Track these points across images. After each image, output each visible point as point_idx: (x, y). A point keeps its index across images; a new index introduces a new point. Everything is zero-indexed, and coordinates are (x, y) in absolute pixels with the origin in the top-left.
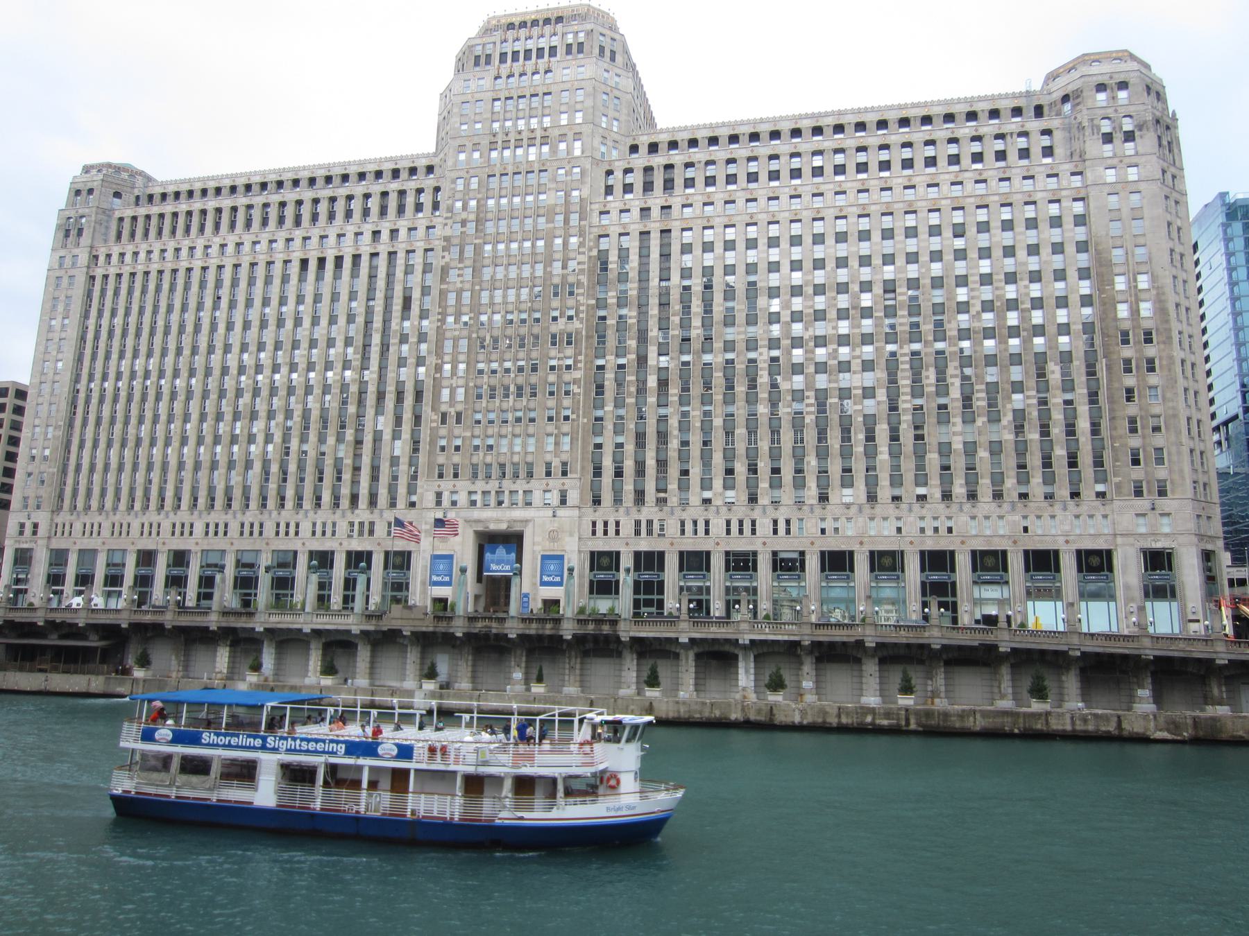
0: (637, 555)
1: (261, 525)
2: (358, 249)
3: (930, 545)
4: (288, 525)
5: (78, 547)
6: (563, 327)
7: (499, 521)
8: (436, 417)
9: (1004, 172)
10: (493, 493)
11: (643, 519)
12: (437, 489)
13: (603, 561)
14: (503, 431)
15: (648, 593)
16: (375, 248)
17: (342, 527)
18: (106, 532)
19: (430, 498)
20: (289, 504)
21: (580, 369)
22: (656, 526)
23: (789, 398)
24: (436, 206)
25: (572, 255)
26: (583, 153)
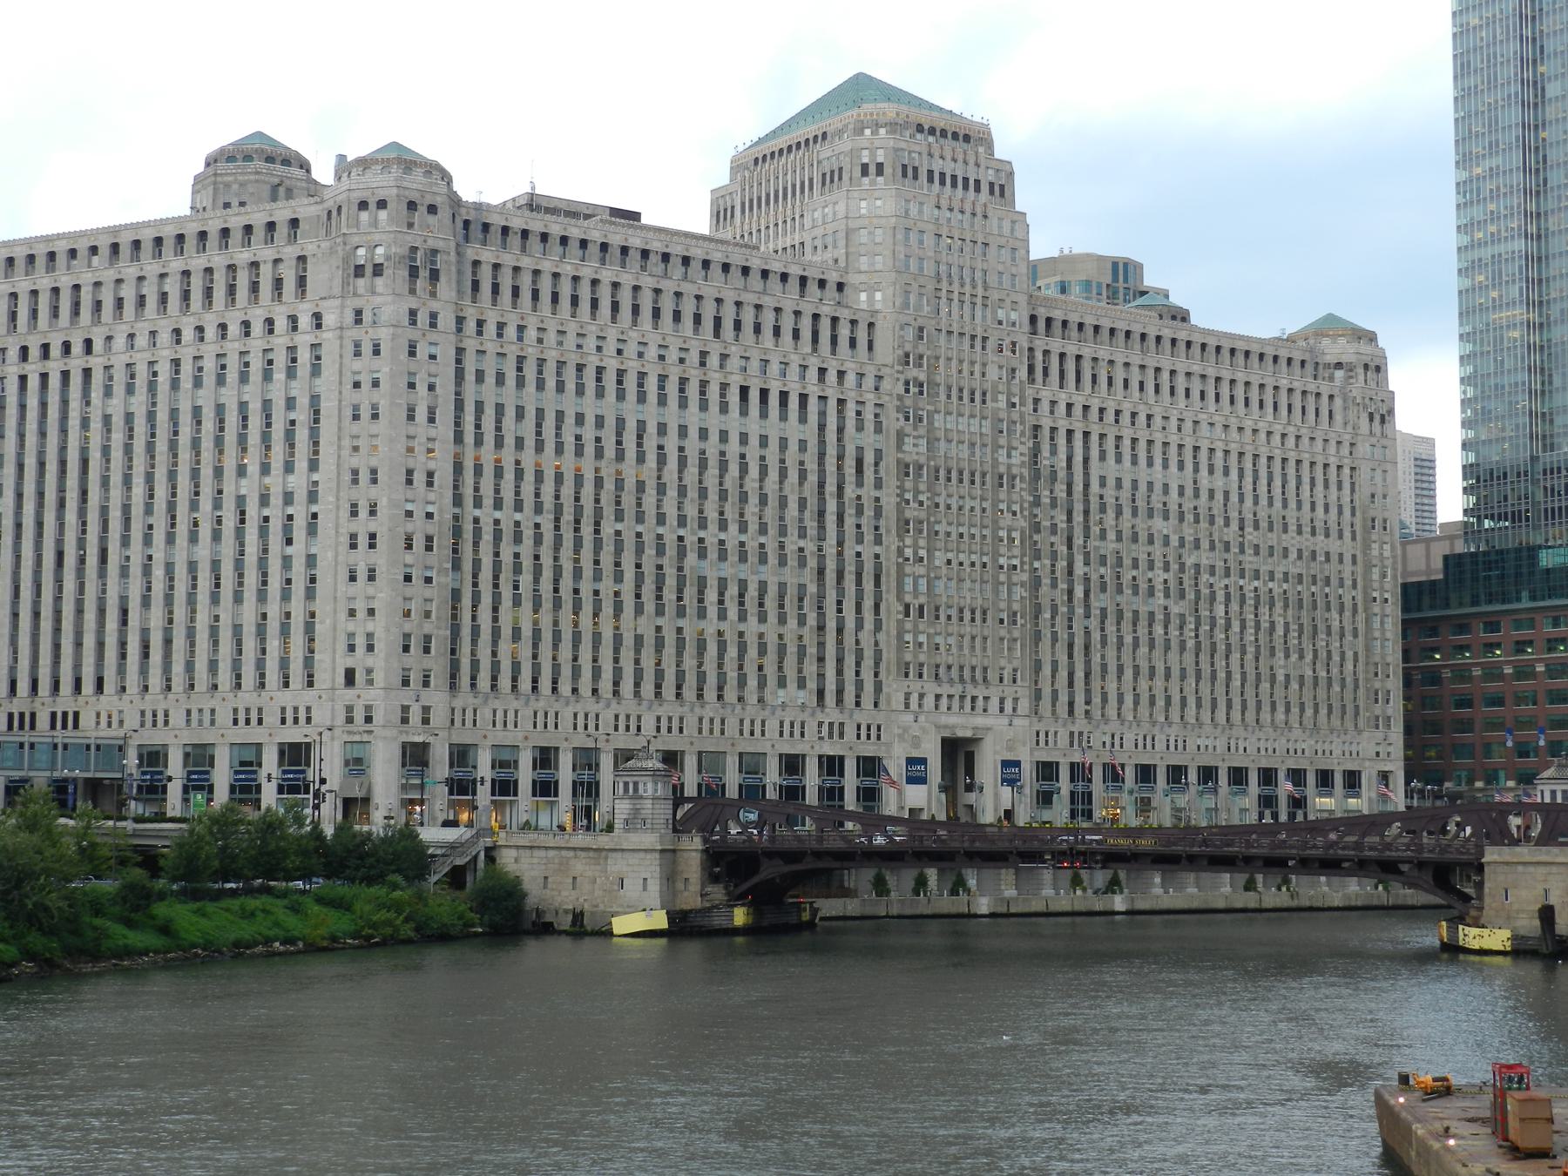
0: (1072, 765)
2: (804, 388)
3: (1264, 764)
5: (489, 742)
10: (957, 697)
11: (1076, 730)
13: (1047, 771)
14: (950, 630)
15: (1082, 804)
16: (823, 390)
19: (898, 700)
22: (1085, 738)
25: (1015, 443)
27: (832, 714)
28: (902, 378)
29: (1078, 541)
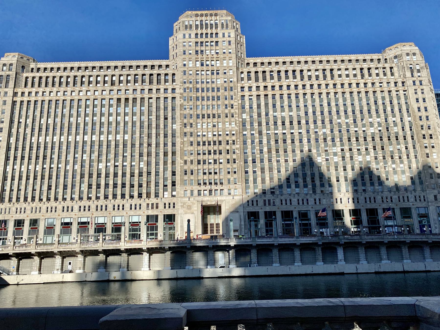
1: (106, 206)
4: (119, 206)
6: (231, 129)
7: (211, 201)
8: (182, 162)
9: (381, 80)
12: (185, 189)
17: (144, 205)
18: (28, 212)
20: (119, 197)
21: (239, 144)
23: (316, 155)
24: (173, 81)
26: (233, 64)
27: (153, 200)
28: (182, 87)
29: (264, 132)
